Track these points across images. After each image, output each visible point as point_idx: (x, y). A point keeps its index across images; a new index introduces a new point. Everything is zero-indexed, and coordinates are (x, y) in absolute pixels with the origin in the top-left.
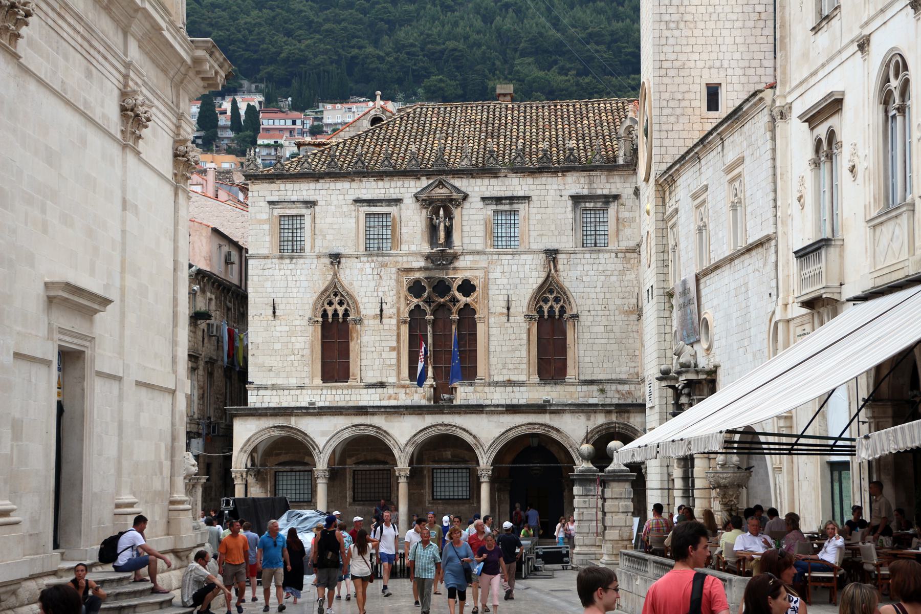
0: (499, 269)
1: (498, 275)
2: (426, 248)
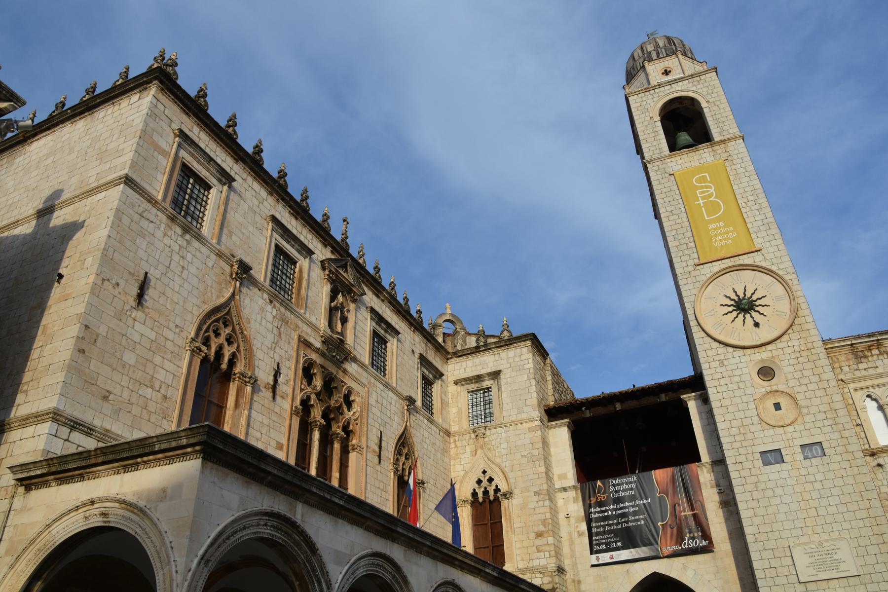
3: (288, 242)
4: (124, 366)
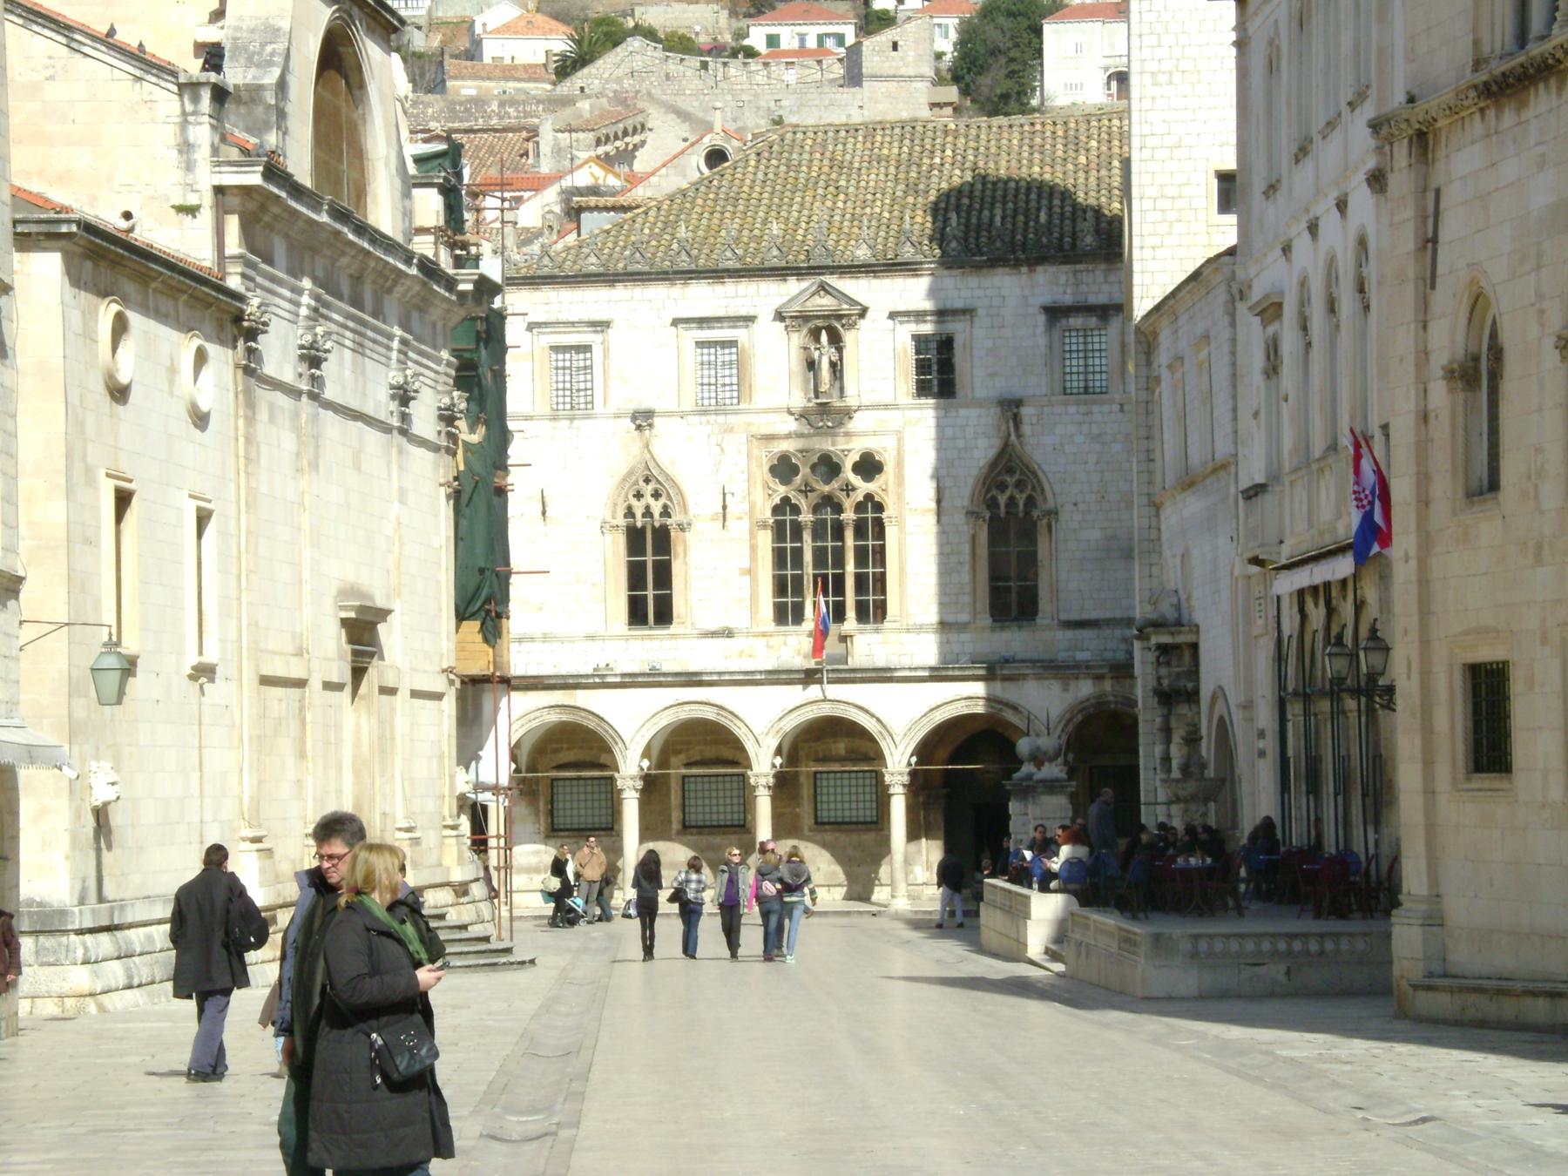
2: (799, 400)
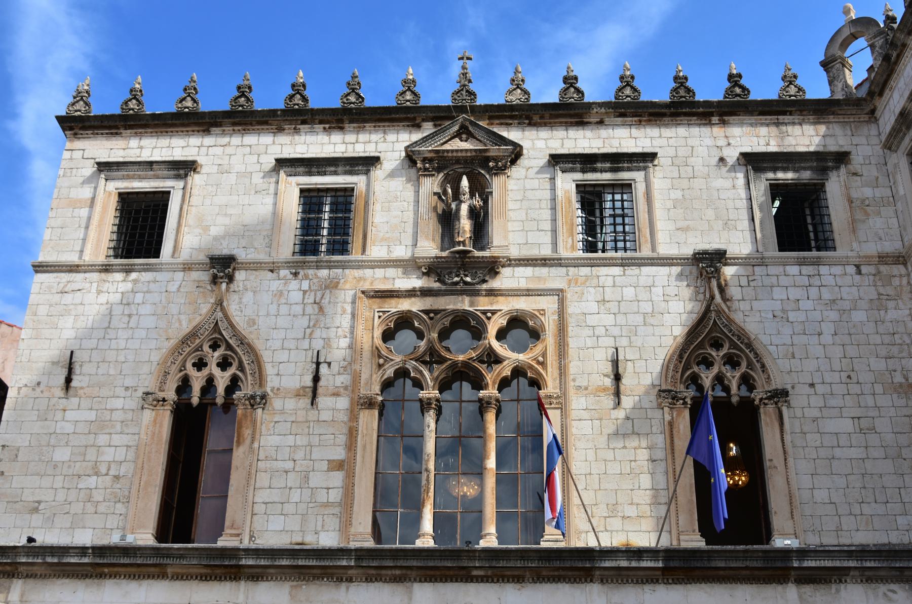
0: (592, 294)
1: (594, 307)
2: (430, 248)
3: (324, 174)
4: (55, 467)
